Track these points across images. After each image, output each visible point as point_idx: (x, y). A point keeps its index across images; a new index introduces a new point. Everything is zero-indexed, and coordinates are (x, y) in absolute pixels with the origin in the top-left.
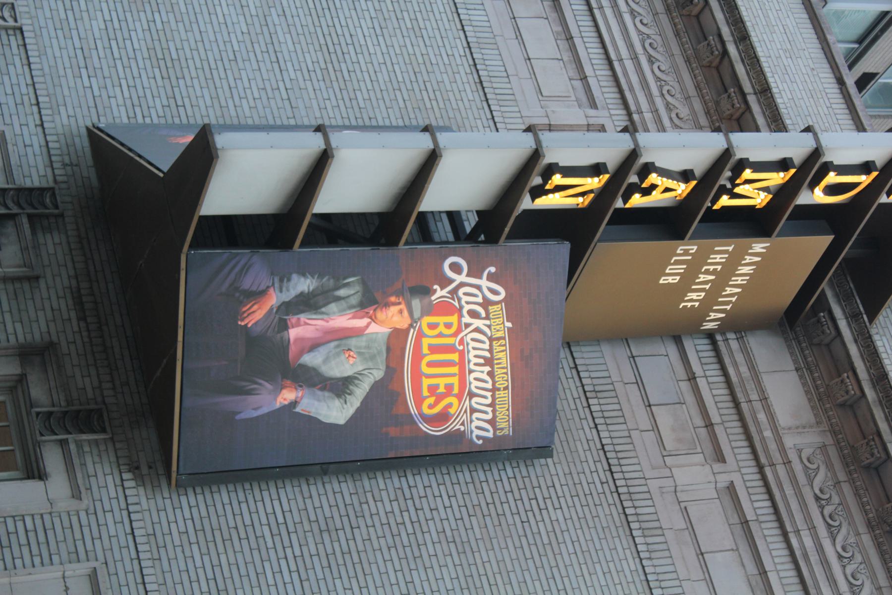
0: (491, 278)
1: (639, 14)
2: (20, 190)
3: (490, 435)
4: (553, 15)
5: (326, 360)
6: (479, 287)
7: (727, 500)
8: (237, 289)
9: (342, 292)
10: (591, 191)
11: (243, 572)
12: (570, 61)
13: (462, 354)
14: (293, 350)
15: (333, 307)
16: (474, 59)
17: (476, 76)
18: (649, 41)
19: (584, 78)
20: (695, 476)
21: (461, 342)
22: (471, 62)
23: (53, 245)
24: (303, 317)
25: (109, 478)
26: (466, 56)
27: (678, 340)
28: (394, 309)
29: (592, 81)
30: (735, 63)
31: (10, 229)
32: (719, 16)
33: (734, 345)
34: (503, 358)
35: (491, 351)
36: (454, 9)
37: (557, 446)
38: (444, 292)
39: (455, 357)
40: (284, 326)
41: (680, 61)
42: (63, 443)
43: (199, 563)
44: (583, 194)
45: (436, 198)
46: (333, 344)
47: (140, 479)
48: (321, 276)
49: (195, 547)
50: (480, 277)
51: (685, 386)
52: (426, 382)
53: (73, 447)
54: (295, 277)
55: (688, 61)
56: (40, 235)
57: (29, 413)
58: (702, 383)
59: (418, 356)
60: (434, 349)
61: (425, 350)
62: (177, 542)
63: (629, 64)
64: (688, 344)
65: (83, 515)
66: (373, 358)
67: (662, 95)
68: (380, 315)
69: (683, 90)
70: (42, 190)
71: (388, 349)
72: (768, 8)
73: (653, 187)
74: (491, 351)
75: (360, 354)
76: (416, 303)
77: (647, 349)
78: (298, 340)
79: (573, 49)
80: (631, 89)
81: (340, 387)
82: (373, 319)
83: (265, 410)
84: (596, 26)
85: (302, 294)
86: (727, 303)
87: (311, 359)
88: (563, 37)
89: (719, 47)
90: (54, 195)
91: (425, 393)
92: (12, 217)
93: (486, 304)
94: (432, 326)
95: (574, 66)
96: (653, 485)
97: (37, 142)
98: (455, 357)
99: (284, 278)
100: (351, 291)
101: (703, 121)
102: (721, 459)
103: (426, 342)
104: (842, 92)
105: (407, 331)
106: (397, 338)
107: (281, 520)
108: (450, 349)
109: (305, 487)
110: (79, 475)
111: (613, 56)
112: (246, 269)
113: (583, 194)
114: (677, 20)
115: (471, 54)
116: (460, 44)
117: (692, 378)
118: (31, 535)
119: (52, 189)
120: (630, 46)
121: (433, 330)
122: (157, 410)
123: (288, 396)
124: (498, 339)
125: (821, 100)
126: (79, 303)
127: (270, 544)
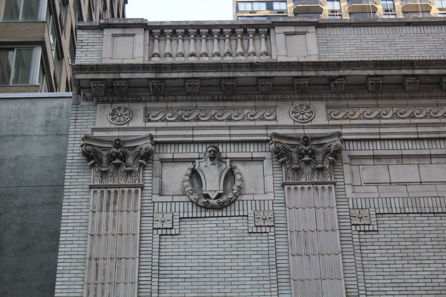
1: (378, 114)
4: (384, 161)
12: (417, 160)
16: (430, 213)
17: (442, 215)
18: (398, 114)
19: (431, 156)
22: (432, 215)
26: (428, 217)
29: (433, 152)
30: (429, 73)
32: (394, 72)
36: (393, 215)
41: (411, 102)
55: (412, 98)
63: (420, 129)
67: (437, 117)
69: (431, 106)
72: (360, 46)
79: (410, 157)
80: (438, 133)
84: (392, 140)
88: (401, 160)
89: (414, 78)
95: (421, 159)
104: (416, 26)
111: (416, 136)
114: (384, 96)
115: (426, 213)
116: (419, 218)
120: (408, 125)
125: (423, 37)
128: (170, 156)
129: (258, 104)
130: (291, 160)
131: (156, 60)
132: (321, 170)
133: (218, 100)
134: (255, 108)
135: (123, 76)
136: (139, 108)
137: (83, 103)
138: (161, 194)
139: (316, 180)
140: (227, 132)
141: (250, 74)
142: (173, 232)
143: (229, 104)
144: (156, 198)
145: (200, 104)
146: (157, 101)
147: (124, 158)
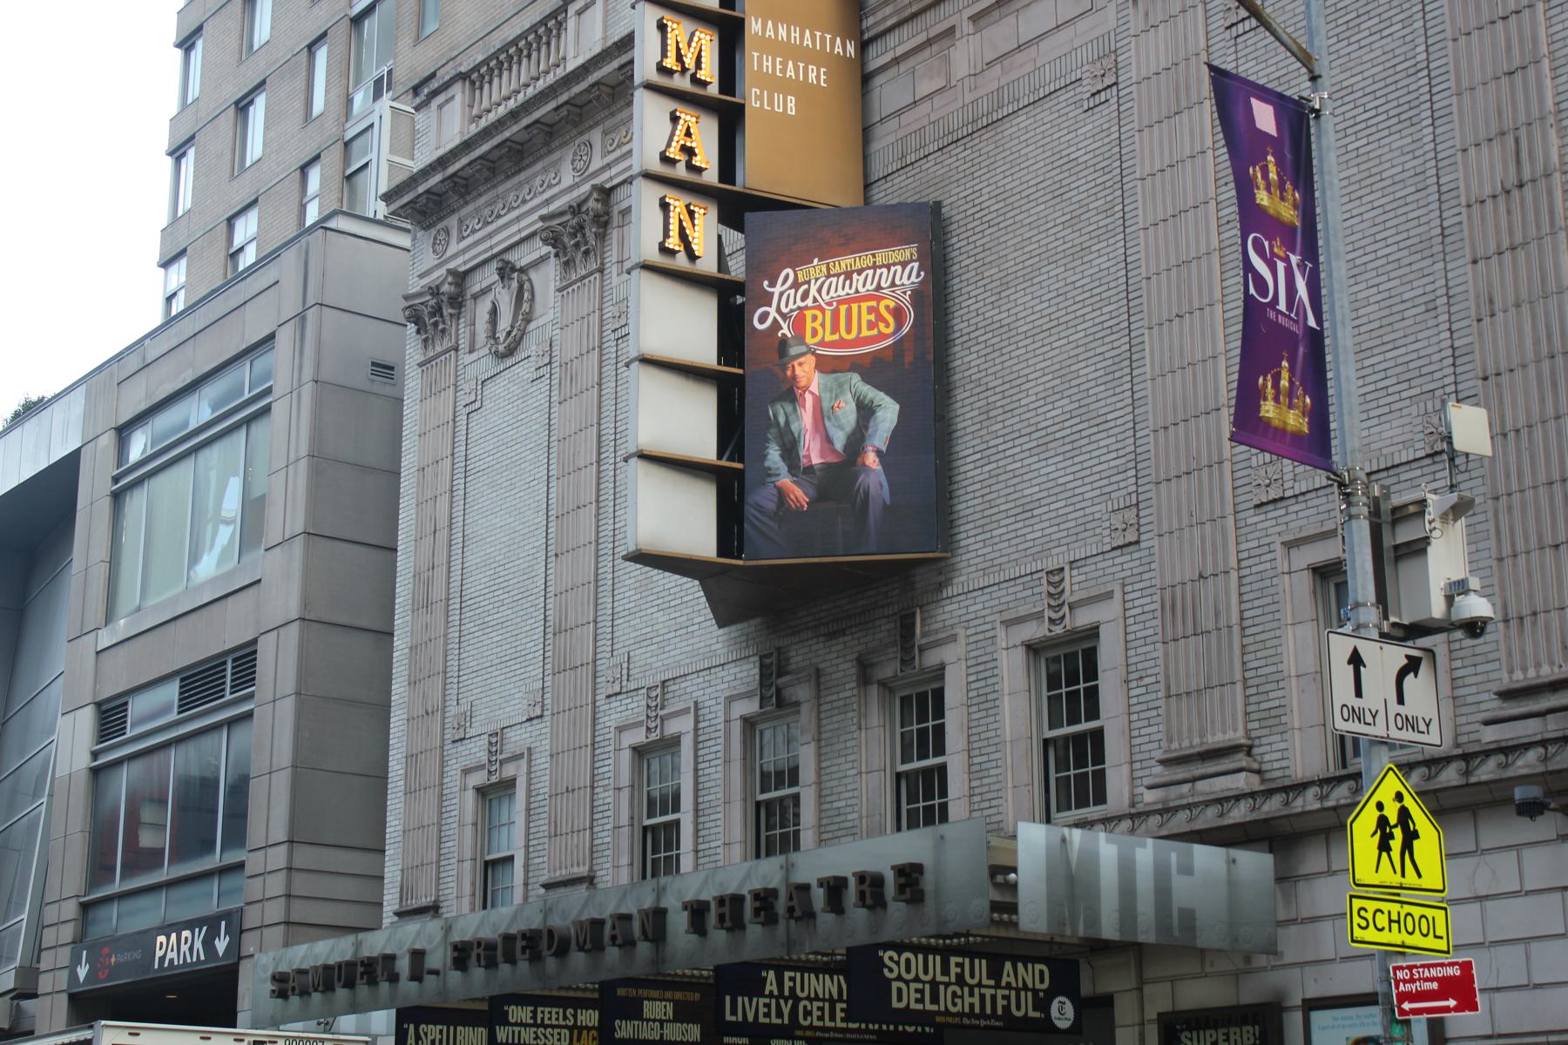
0: (773, 285)
2: (761, 684)
3: (916, 265)
5: (841, 428)
6: (781, 294)
7: (983, 22)
8: (776, 514)
9: (782, 420)
10: (687, 206)
11: (1011, 490)
13: (840, 302)
14: (831, 459)
15: (794, 427)
20: (964, 55)
21: (829, 304)
23: (799, 657)
24: (802, 453)
25: (947, 609)
27: (866, 79)
28: (799, 371)
31: (786, 693)
33: (871, 21)
34: (846, 262)
35: (838, 275)
37: (931, 198)
38: (785, 326)
39: (843, 308)
40: (810, 469)
42: (921, 650)
43: (1004, 530)
44: (691, 214)
45: (703, 348)
46: (827, 423)
47: (948, 582)
48: (767, 440)
49: (995, 533)
50: (772, 294)
51: (903, 67)
52: (865, 333)
53: (923, 641)
54: (767, 464)
56: (793, 667)
57: (903, 678)
58: (900, 51)
59: (842, 343)
60: (835, 329)
61: (836, 337)
62: (989, 549)
64: (873, 65)
65: (970, 632)
66: (840, 385)
68: (803, 383)
70: (762, 666)
71: (834, 371)
73: (684, 149)
74: (838, 275)
75: (837, 397)
76: (793, 351)
77: (876, 104)
78: (822, 456)
81: (866, 411)
82: (806, 389)
83: (883, 479)
85: (782, 456)
86: (823, 39)
87: (839, 441)
90: (766, 656)
91: (875, 332)
92: (779, 691)
93: (796, 285)
94: (815, 333)
96: (968, 98)
97: (733, 669)
98: (843, 308)
99: (768, 473)
100: (780, 412)
101: (624, 114)
102: (951, 31)
103: (829, 338)
105: (818, 356)
106: (824, 365)
107: (978, 456)
108: (836, 314)
109: (959, 434)
110: (941, 636)
112: (759, 508)
113: (691, 214)
117: (896, 61)
118: (981, 676)
119: (761, 658)
121: (818, 332)
122: (904, 569)
123: (871, 459)
124: (828, 269)
126: (832, 636)
127: (994, 465)
128: (476, 288)
129: (547, 161)
130: (565, 248)
131: (474, 129)
132: (586, 253)
133: (513, 175)
134: (545, 170)
135: (421, 189)
136: (452, 222)
137: (420, 234)
138: (471, 352)
139: (584, 272)
140: (514, 228)
141: (515, 128)
142: (478, 404)
143: (522, 176)
144: (469, 358)
145: (501, 189)
146: (467, 203)
147: (437, 311)
